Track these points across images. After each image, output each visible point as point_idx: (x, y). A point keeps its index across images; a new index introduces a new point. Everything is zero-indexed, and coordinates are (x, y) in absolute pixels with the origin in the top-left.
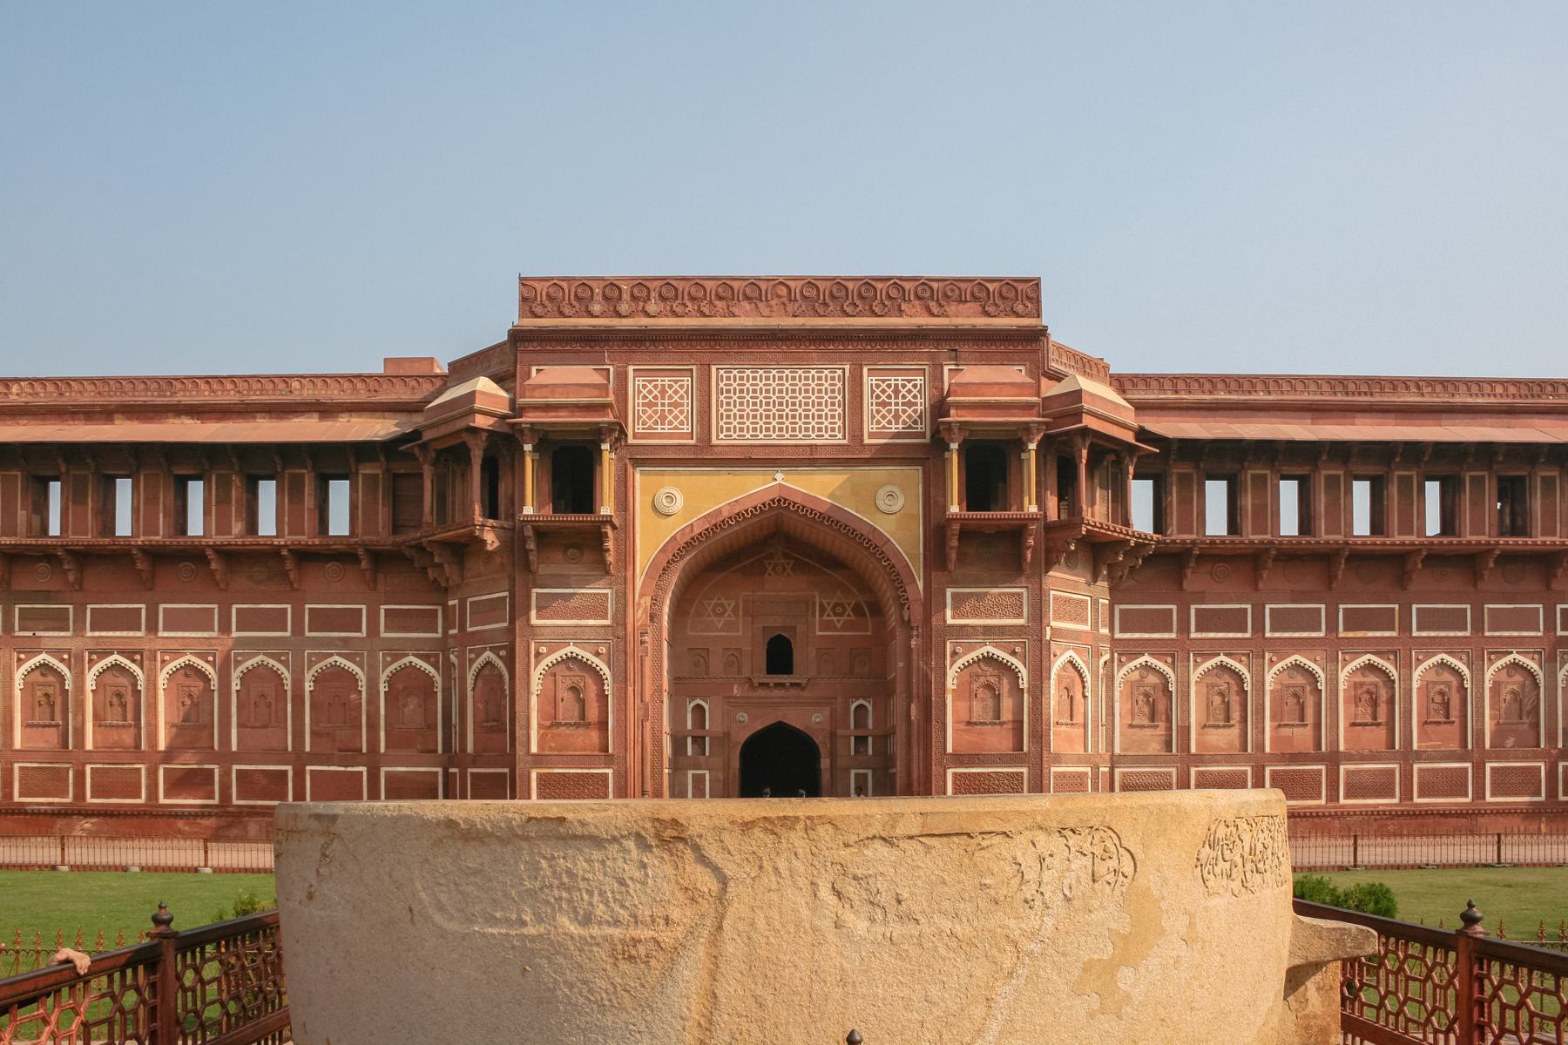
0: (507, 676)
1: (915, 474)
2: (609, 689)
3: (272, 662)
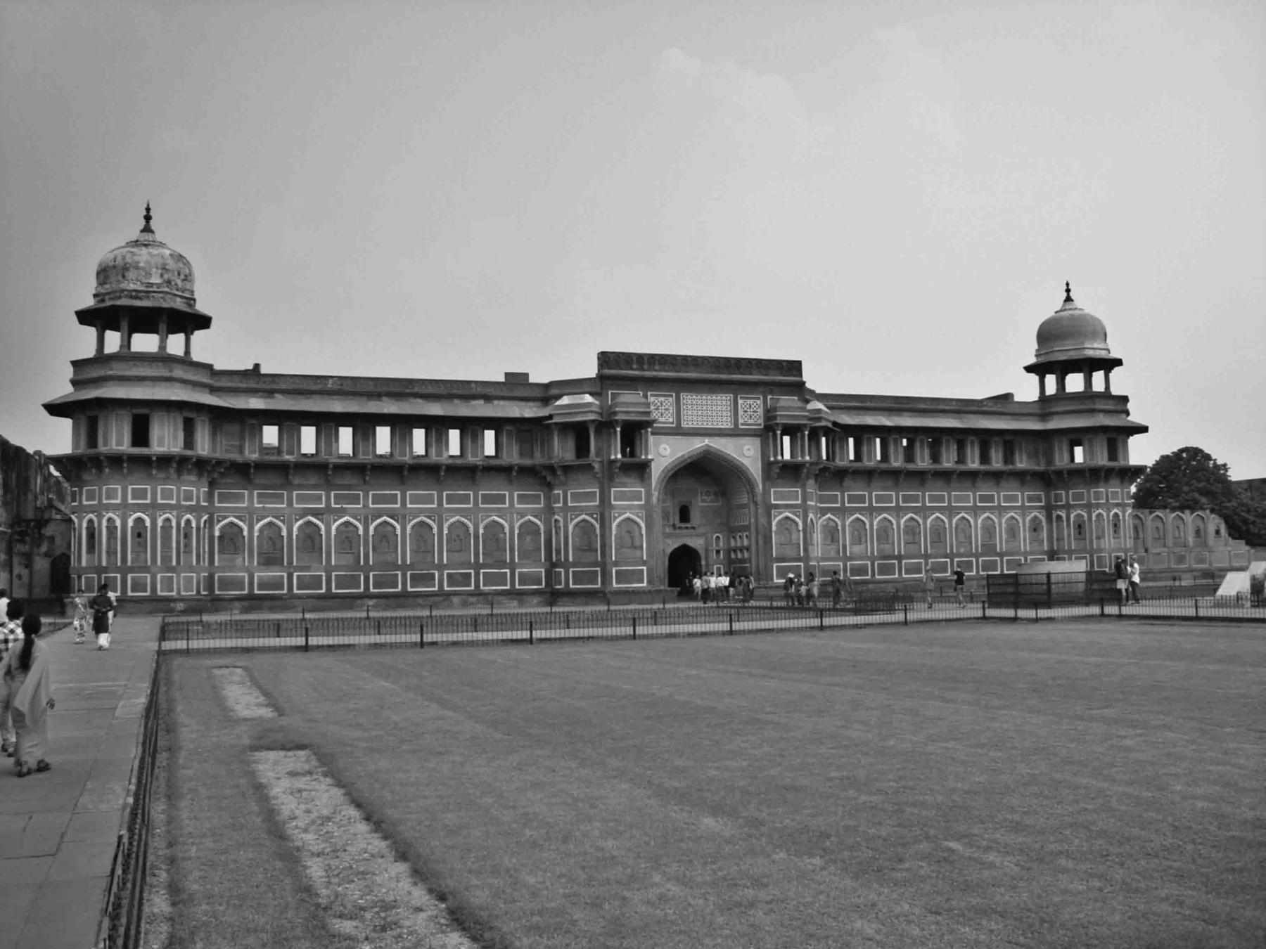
0: (598, 526)
1: (757, 441)
2: (644, 532)
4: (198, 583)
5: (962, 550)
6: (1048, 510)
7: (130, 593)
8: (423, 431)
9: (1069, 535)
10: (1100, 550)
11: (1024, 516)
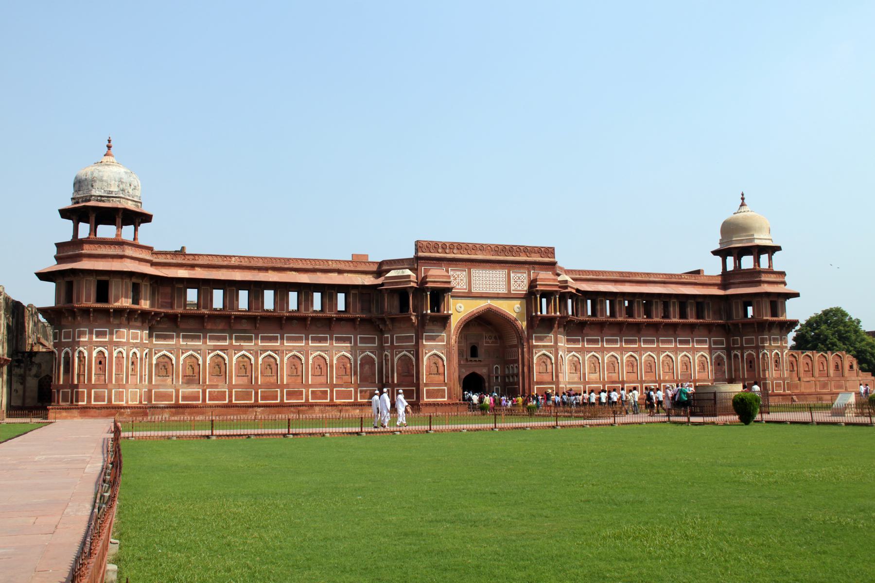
0: (414, 359)
1: (524, 301)
2: (445, 363)
3: (323, 354)
4: (141, 396)
5: (667, 378)
6: (728, 350)
7: (93, 403)
8: (296, 293)
9: (743, 368)
10: (765, 379)
11: (711, 354)
